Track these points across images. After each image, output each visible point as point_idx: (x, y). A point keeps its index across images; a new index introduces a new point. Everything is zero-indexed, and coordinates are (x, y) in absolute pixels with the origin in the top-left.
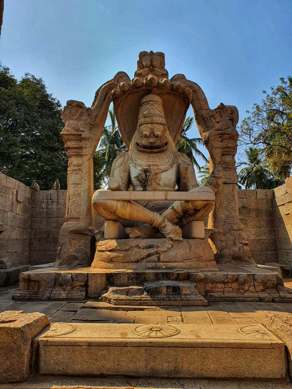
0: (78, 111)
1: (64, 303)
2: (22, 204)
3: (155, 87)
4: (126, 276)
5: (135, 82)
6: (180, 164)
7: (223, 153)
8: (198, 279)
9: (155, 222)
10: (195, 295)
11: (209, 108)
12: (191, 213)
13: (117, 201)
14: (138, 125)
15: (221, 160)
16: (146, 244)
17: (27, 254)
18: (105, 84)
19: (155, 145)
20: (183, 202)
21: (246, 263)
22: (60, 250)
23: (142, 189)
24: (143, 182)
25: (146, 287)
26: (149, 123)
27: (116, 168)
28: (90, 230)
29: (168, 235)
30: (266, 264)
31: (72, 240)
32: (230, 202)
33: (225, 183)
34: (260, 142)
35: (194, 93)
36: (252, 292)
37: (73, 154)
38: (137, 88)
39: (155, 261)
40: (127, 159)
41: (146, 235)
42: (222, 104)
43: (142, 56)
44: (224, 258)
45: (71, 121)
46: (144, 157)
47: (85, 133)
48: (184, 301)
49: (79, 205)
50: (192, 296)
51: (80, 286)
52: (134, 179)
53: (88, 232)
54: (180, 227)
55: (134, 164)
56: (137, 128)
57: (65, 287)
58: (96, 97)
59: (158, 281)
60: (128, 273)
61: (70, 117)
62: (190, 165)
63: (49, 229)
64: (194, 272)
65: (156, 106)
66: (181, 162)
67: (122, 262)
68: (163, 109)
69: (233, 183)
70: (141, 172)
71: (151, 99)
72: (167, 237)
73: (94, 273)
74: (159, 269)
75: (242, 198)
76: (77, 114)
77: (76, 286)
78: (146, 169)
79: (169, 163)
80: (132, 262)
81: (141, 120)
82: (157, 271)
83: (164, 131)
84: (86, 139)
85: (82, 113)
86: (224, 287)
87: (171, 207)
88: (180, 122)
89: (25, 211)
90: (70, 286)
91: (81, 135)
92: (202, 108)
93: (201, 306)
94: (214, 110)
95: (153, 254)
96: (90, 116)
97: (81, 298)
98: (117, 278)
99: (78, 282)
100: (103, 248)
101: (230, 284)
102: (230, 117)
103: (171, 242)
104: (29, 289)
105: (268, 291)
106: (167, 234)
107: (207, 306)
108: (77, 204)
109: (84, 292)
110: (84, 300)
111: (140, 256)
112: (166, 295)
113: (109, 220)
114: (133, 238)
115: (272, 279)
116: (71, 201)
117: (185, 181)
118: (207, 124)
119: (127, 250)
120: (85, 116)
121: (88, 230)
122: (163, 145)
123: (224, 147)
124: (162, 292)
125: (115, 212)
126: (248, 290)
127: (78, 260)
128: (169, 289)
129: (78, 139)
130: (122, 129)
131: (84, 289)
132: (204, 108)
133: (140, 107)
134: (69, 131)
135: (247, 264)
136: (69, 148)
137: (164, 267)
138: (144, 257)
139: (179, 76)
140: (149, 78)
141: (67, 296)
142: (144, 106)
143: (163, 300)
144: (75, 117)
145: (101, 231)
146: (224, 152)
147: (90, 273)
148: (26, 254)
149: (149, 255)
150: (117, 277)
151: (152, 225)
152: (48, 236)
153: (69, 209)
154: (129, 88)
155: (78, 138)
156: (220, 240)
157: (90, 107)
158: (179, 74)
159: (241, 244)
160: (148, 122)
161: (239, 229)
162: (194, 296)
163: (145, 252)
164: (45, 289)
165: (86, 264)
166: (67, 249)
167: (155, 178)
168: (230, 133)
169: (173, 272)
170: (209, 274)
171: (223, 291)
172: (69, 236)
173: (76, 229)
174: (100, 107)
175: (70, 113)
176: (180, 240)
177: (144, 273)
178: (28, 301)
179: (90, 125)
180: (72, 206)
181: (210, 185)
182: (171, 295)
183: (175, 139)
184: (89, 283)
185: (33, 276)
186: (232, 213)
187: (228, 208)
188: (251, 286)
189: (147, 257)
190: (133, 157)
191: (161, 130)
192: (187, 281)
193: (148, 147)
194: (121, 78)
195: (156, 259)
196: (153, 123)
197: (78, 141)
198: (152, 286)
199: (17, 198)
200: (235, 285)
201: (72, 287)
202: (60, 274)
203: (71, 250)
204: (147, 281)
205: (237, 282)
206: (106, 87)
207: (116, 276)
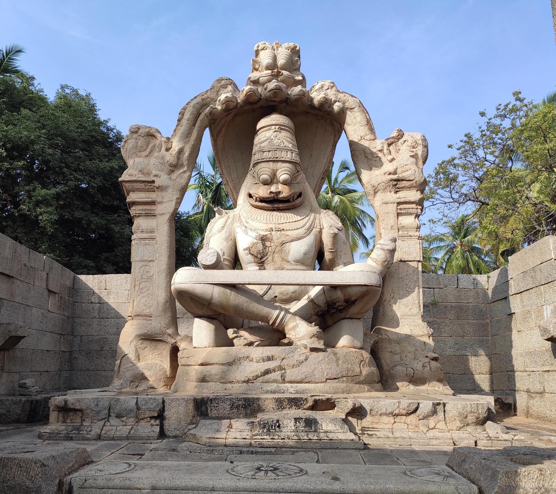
1: (124, 443)
12: (341, 306)
16: (261, 354)
24: (259, 256)
27: (214, 234)
34: (470, 200)
46: (262, 216)
51: (151, 418)
52: (243, 252)
54: (320, 328)
55: (244, 228)
56: (250, 169)
57: (127, 419)
59: (283, 409)
70: (255, 241)
73: (174, 399)
74: (283, 393)
76: (147, 148)
77: (145, 418)
78: (263, 235)
87: (306, 297)
91: (153, 182)
95: (274, 371)
96: (170, 151)
97: (153, 437)
99: (148, 412)
104: (66, 423)
122: (293, 197)
129: (148, 189)
130: (224, 171)
131: (158, 422)
134: (134, 175)
136: (134, 203)
137: (291, 390)
138: (259, 374)
141: (129, 433)
142: (262, 134)
149: (267, 372)
154: (235, 104)
160: (268, 159)
164: (91, 423)
167: (281, 251)
171: (392, 429)
176: (320, 349)
178: (64, 440)
183: (315, 190)
189: (264, 375)
190: (242, 216)
193: (268, 200)
195: (279, 378)
196: (278, 161)
201: (137, 420)
202: (118, 399)
207: (211, 403)
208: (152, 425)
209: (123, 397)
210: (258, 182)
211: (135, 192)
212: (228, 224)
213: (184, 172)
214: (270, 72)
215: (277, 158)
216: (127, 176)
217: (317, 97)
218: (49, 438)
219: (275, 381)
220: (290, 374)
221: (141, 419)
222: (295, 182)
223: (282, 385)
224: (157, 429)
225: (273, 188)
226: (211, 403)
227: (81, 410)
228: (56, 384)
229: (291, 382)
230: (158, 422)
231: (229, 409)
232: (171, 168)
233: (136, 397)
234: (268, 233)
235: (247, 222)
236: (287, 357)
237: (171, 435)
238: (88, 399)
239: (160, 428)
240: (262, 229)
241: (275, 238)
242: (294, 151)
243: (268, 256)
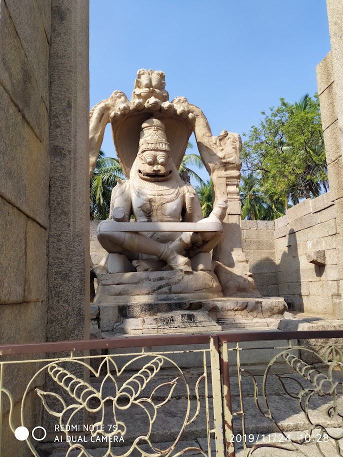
3: (156, 111)
7: (227, 182)
9: (164, 254)
13: (124, 233)
20: (192, 233)
24: (148, 212)
27: (116, 197)
33: (229, 214)
38: (138, 111)
39: (166, 293)
41: (153, 267)
51: (92, 319)
56: (138, 153)
65: (160, 132)
82: (170, 302)
83: (167, 158)
86: (234, 314)
87: (178, 239)
101: (240, 312)
105: (275, 316)
112: (181, 323)
113: (114, 253)
114: (141, 271)
131: (96, 322)
137: (175, 298)
149: (160, 287)
151: (160, 257)
181: (216, 215)
195: (168, 291)
208: (93, 324)
213: (94, 153)
214: (147, 89)
217: (179, 109)
220: (174, 288)
223: (169, 295)
225: (155, 168)
229: (175, 293)
230: (96, 322)
234: (153, 197)
241: (157, 200)
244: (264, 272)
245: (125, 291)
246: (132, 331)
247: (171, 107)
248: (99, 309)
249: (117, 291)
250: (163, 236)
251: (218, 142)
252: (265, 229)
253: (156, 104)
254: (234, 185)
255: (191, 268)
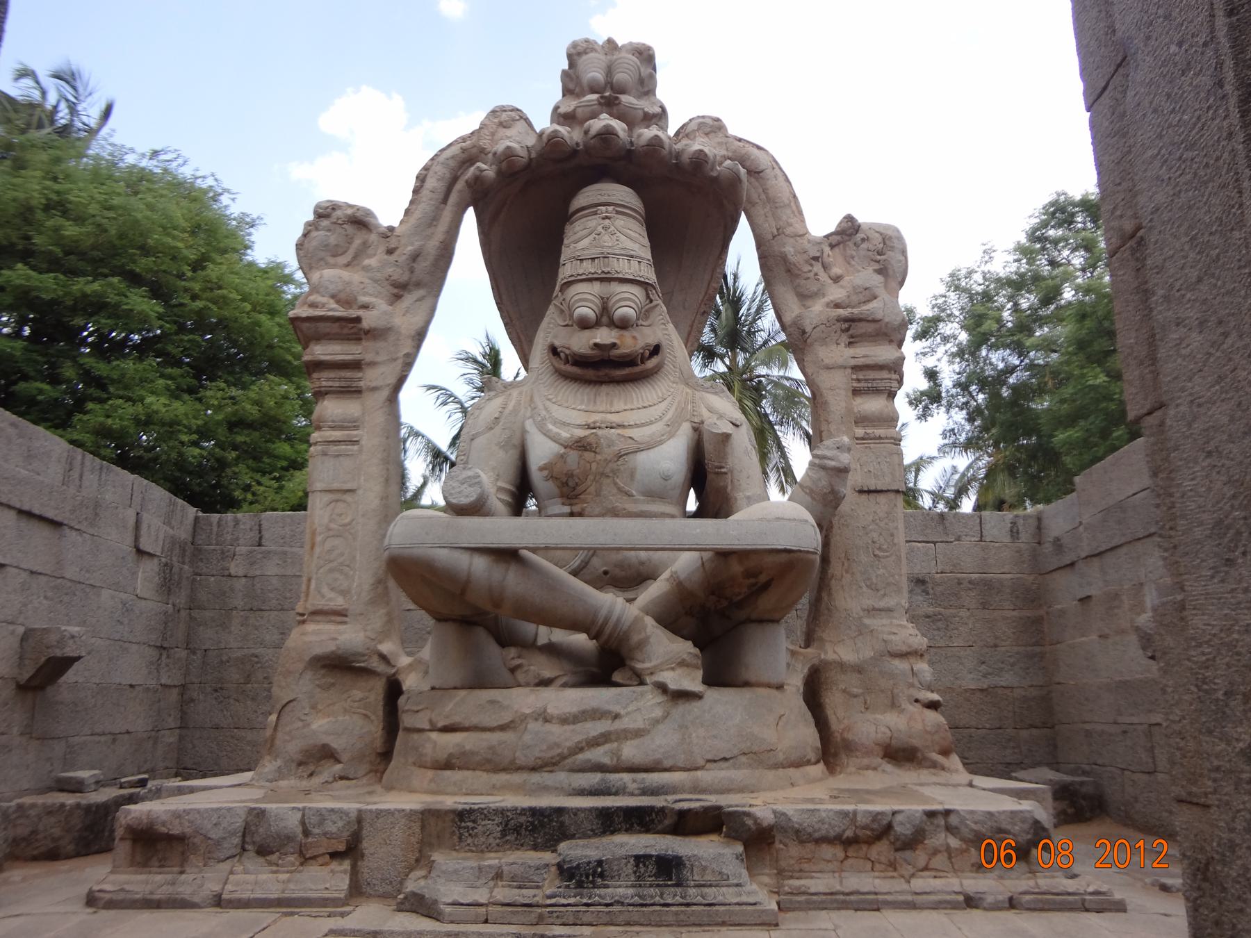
0: (352, 238)
2: (156, 561)
4: (498, 820)
5: (549, 140)
6: (702, 422)
7: (855, 385)
8: (750, 829)
9: (608, 630)
10: (737, 885)
11: (807, 232)
13: (469, 552)
14: (557, 288)
15: (849, 410)
17: (172, 740)
18: (450, 145)
19: (614, 352)
20: (707, 555)
21: (932, 770)
22: (276, 726)
23: (567, 509)
25: (564, 861)
26: (596, 279)
28: (383, 658)
29: (652, 673)
30: (1014, 774)
31: (319, 690)
32: (881, 554)
33: (861, 492)
35: (757, 179)
36: (938, 873)
37: (330, 384)
40: (518, 403)
41: (575, 673)
42: (849, 219)
43: (579, 54)
44: (858, 753)
45: (328, 273)
47: (375, 312)
48: (694, 908)
49: (348, 566)
50: (724, 889)
53: (375, 664)
54: (695, 645)
56: (555, 295)
58: (416, 191)
59: (612, 833)
60: (502, 812)
61: (322, 259)
62: (737, 426)
63: (253, 651)
64: (737, 806)
65: (620, 222)
66: (705, 413)
67: (484, 771)
68: (645, 234)
69: (888, 491)
70: (562, 450)
71: (603, 199)
72: (648, 682)
73: (381, 811)
74: (616, 794)
75: (932, 542)
76: (348, 248)
78: (580, 440)
79: (666, 419)
80: (520, 769)
81: (567, 270)
84: (373, 334)
85: (365, 245)
88: (707, 277)
89: (167, 584)
90: (296, 855)
91: (358, 320)
92: (780, 231)
93: (756, 925)
94: (825, 237)
98: (465, 828)
100: (421, 721)
101: (864, 847)
102: (878, 262)
103: (660, 698)
106: (649, 672)
107: (777, 925)
108: (342, 564)
109: (344, 876)
110: (343, 906)
111: (550, 748)
114: (528, 685)
115: (1009, 827)
116: (317, 550)
117: (722, 484)
118: (799, 285)
119: (502, 728)
120: (375, 255)
121: (375, 658)
122: (642, 354)
123: (860, 364)
124: (619, 875)
125: (463, 591)
126: (926, 869)
127: (340, 762)
128: (644, 865)
130: (504, 297)
132: (787, 233)
133: (567, 227)
135: (934, 774)
136: (319, 366)
137: (632, 787)
138: (566, 751)
139: (701, 123)
140: (593, 131)
141: (283, 892)
143: (622, 904)
144: (343, 260)
145: (419, 662)
146: (858, 380)
147: (370, 807)
148: (170, 738)
150: (463, 824)
152: (249, 676)
153: (309, 580)
155: (352, 331)
156: (844, 691)
157: (396, 224)
158: (703, 117)
159: (917, 705)
161: (909, 650)
162: (731, 890)
163: (567, 736)
165: (368, 776)
166: (300, 724)
167: (615, 472)
168: (879, 316)
169: (664, 804)
170: (789, 809)
172: (309, 675)
173: (333, 652)
174: (430, 225)
175: (326, 246)
177: (560, 811)
179: (392, 285)
180: (322, 570)
182: (651, 886)
183: (689, 334)
184: (364, 842)
185: (164, 817)
186: (884, 595)
187: (874, 580)
188: (936, 852)
189: (577, 754)
191: (635, 303)
192: (714, 837)
194: (505, 127)
197: (348, 339)
198: (586, 856)
199: (137, 538)
200: (881, 850)
203: (314, 726)
204: (572, 837)
205: (888, 839)
206: (453, 157)
209: (274, 806)
210: (570, 323)
211: (323, 341)
212: (507, 411)
213: (420, 300)
215: (609, 273)
216: (305, 308)
218: (111, 905)
219: (601, 768)
221: (311, 858)
222: (644, 323)
224: (343, 883)
226: (462, 820)
227: (181, 839)
228: (145, 762)
231: (499, 835)
232: (395, 291)
233: (300, 805)
235: (546, 409)
236: (622, 712)
237: (373, 893)
238: (198, 811)
239: (351, 880)
240: (578, 423)
242: (643, 259)
243: (589, 482)
244: (1002, 684)
245: (464, 754)
246: (448, 909)
247: (656, 143)
248: (359, 821)
249: (442, 756)
250: (620, 565)
251: (827, 249)
252: (1007, 539)
253: (607, 135)
254: (876, 391)
255: (699, 674)
